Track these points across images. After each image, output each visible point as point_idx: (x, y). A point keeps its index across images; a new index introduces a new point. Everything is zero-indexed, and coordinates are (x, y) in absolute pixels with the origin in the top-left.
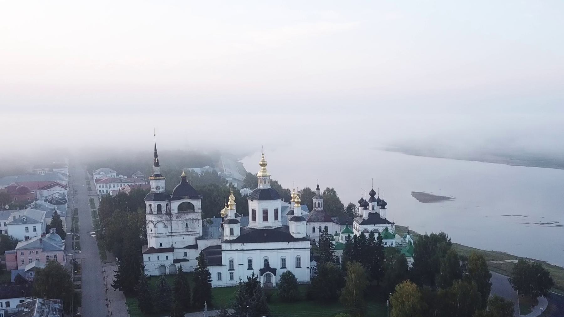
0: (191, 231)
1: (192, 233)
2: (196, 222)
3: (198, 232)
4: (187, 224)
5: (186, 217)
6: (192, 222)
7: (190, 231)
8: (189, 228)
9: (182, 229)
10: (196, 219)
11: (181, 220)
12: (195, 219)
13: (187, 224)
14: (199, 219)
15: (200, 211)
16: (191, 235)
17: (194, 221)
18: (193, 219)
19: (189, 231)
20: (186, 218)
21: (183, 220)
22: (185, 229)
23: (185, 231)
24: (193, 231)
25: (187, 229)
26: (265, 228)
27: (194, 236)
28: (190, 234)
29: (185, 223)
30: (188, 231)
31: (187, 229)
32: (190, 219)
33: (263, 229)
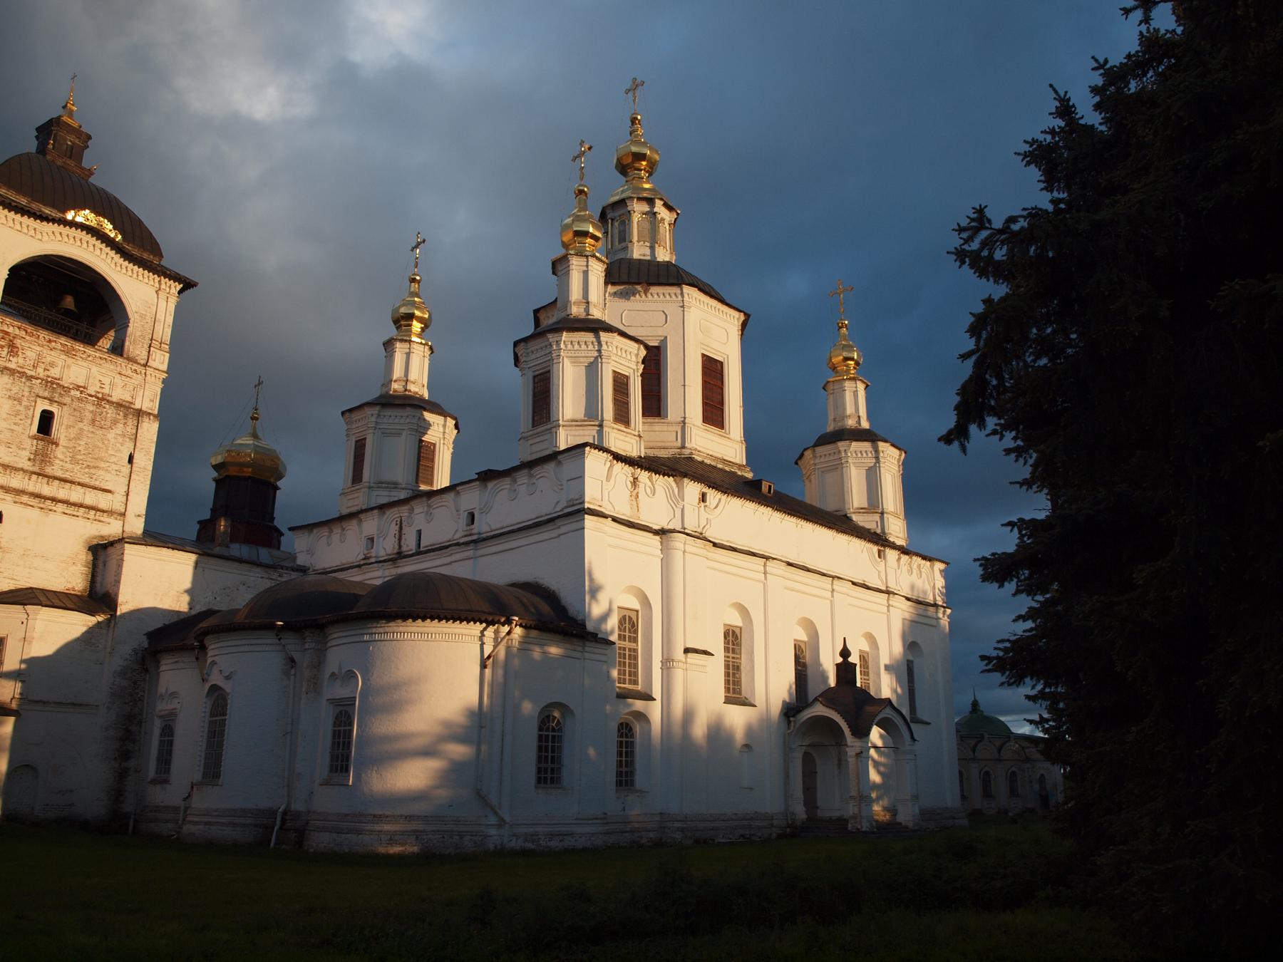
0: (67, 476)
1: (76, 494)
2: (115, 422)
3: (115, 502)
4: (46, 421)
5: (52, 365)
6: (89, 416)
7: (65, 481)
8: (59, 452)
9: (8, 445)
10: (119, 405)
11: (12, 372)
12: (114, 399)
13: (46, 421)
14: (139, 413)
15: (161, 360)
16: (60, 507)
17: (110, 412)
18: (102, 400)
19: (59, 474)
20: (55, 372)
21: (30, 378)
22: (30, 445)
23: (27, 465)
24: (86, 480)
25: (42, 457)
26: (720, 466)
27: (81, 522)
28: (54, 500)
29: (43, 405)
30: (49, 470)
31: (42, 457)
32: (78, 387)
33: (713, 463)
